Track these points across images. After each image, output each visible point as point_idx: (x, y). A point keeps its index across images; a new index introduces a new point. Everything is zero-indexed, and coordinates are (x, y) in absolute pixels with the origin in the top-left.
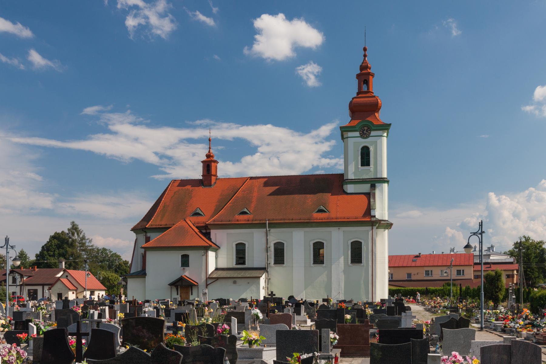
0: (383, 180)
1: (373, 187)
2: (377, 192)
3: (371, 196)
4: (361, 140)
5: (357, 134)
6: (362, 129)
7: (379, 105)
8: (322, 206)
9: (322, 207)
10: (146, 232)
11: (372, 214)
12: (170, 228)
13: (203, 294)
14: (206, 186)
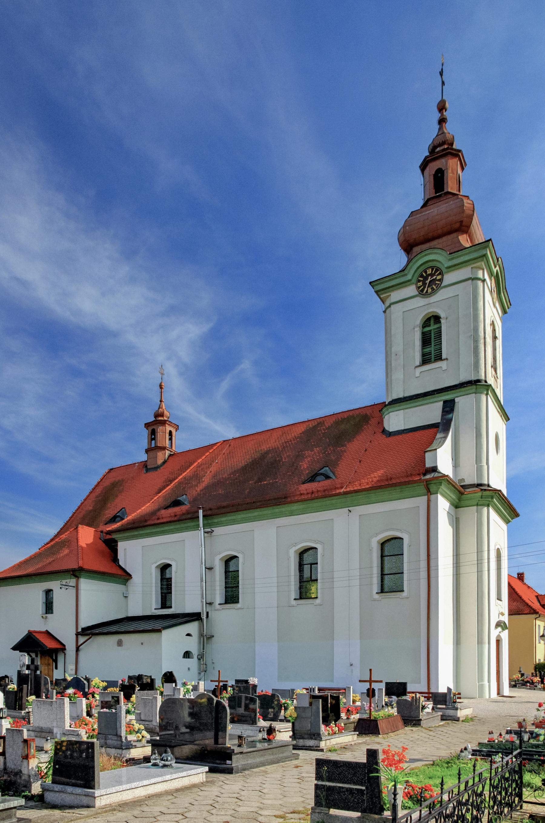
5: (411, 290)
6: (421, 276)
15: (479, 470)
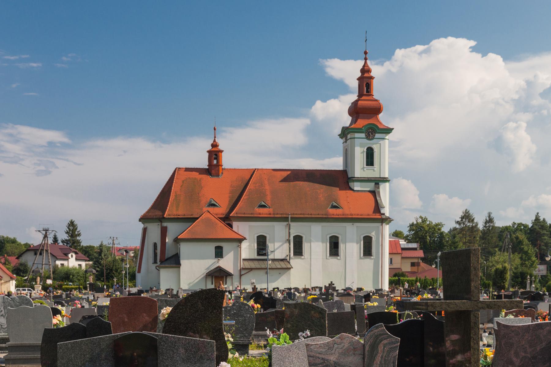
0: (385, 180)
2: (381, 190)
3: (377, 194)
4: (366, 141)
5: (363, 135)
6: (367, 131)
7: (381, 109)
8: (334, 202)
9: (335, 204)
10: (161, 222)
11: (382, 212)
12: (197, 218)
13: (251, 283)
14: (214, 176)
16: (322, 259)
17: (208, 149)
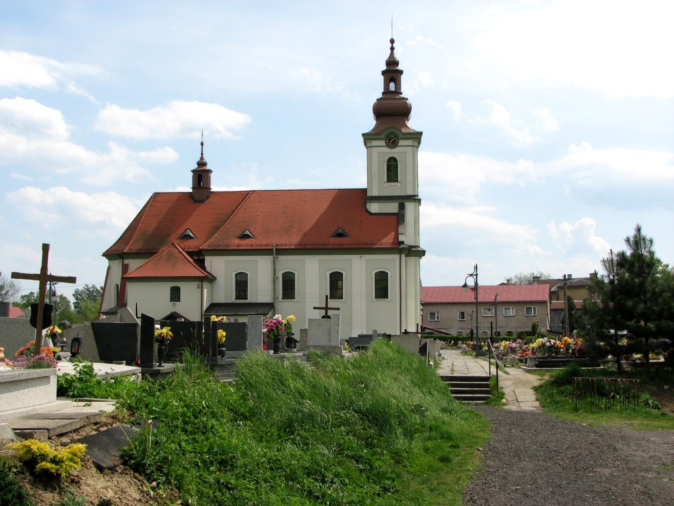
1: (402, 207)
4: (387, 150)
5: (383, 143)
15: (415, 239)
16: (320, 302)
17: (193, 169)
